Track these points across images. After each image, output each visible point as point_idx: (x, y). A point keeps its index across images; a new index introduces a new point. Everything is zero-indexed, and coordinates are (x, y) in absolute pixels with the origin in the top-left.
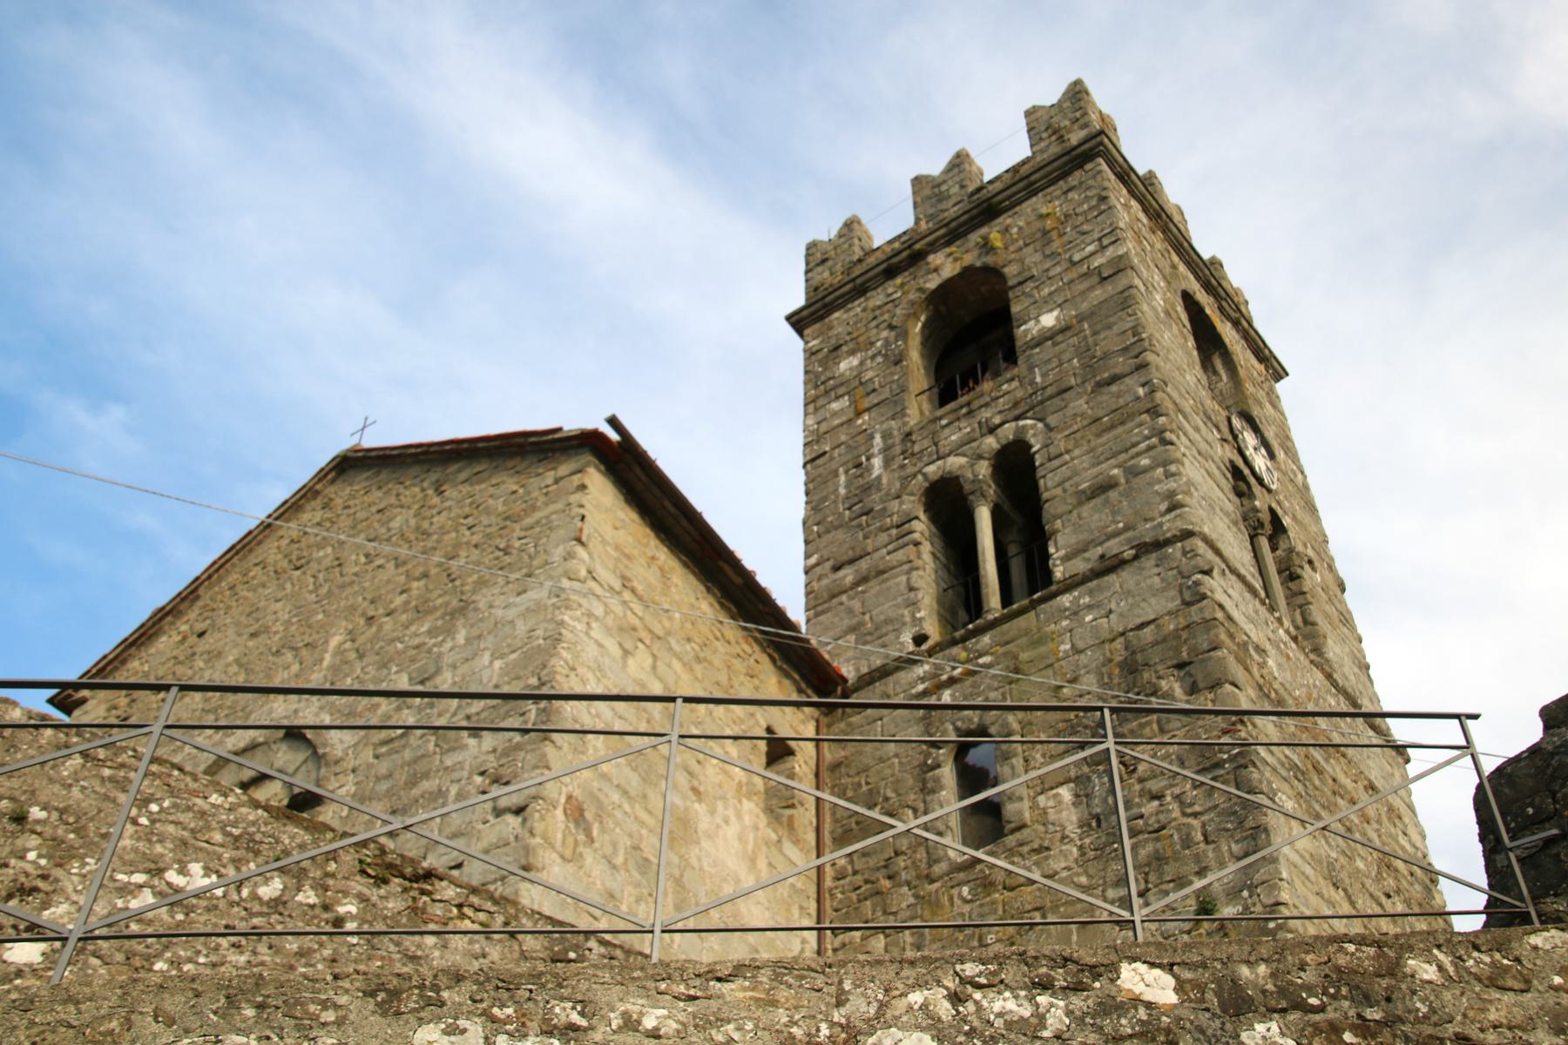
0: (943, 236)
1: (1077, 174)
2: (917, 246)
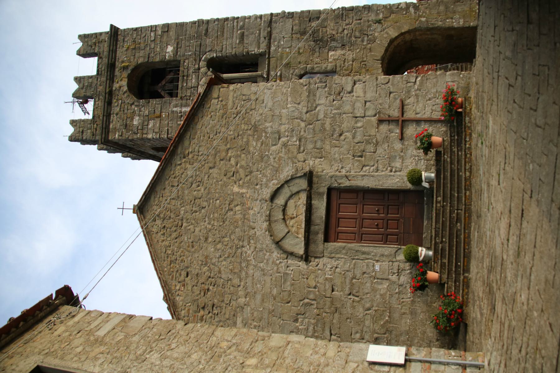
0: (110, 82)
1: (119, 37)
2: (107, 90)
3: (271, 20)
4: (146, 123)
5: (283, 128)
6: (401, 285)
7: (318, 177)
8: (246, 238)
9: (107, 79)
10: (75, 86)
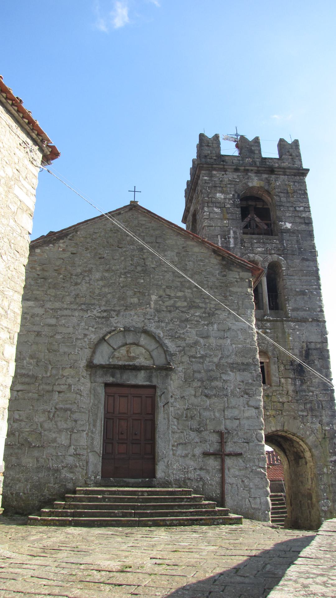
3: (318, 321)
4: (218, 205)
5: (212, 340)
6: (64, 458)
7: (167, 375)
8: (109, 308)
9: (258, 167)
10: (250, 138)
